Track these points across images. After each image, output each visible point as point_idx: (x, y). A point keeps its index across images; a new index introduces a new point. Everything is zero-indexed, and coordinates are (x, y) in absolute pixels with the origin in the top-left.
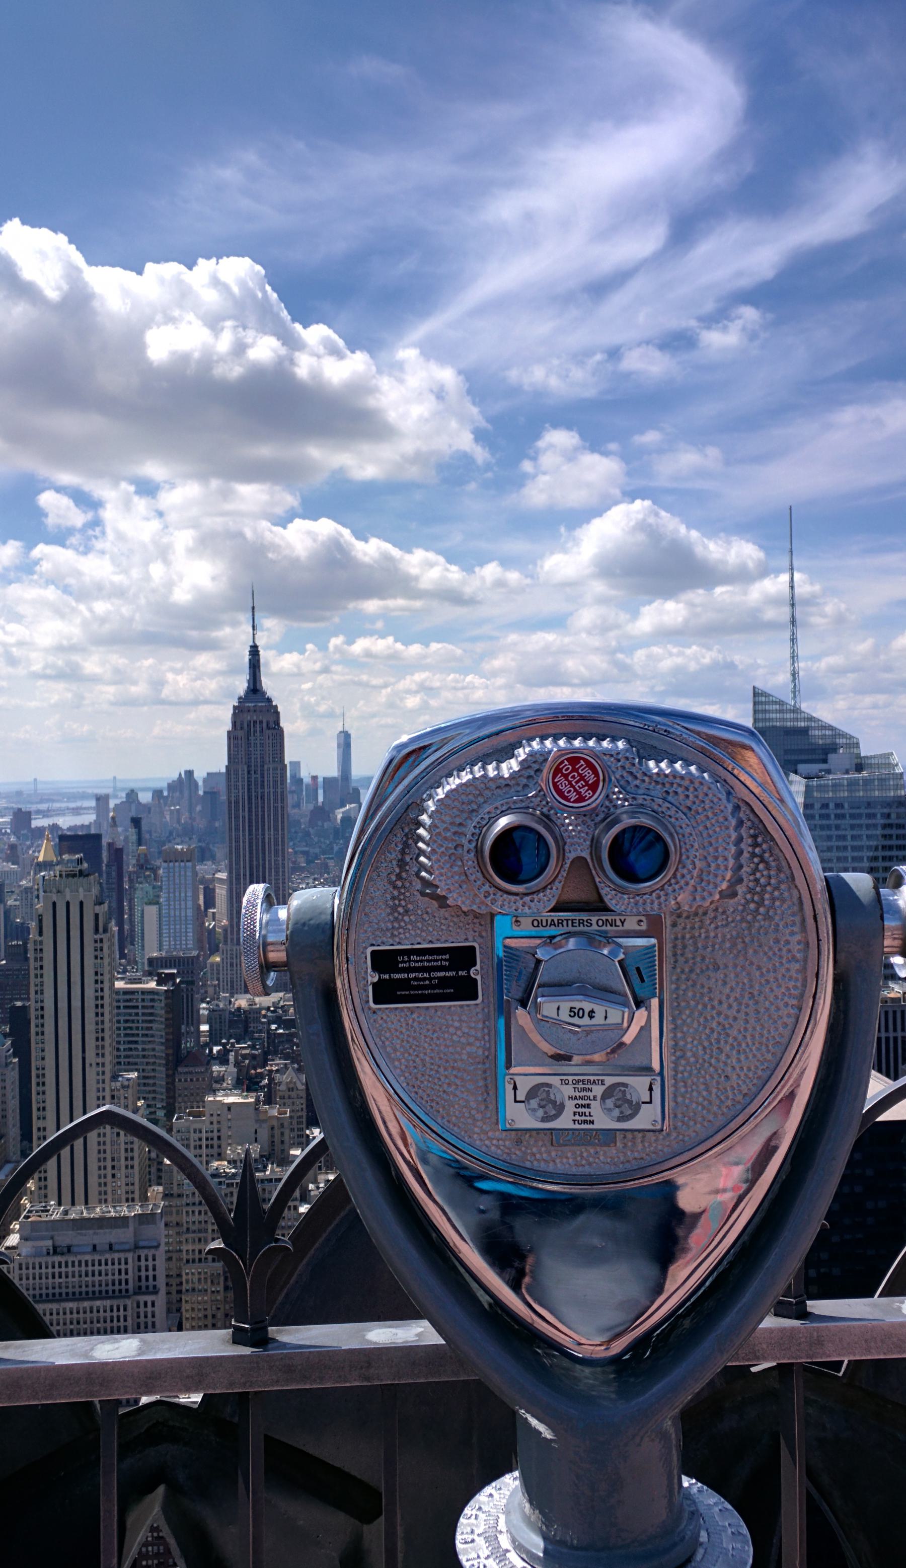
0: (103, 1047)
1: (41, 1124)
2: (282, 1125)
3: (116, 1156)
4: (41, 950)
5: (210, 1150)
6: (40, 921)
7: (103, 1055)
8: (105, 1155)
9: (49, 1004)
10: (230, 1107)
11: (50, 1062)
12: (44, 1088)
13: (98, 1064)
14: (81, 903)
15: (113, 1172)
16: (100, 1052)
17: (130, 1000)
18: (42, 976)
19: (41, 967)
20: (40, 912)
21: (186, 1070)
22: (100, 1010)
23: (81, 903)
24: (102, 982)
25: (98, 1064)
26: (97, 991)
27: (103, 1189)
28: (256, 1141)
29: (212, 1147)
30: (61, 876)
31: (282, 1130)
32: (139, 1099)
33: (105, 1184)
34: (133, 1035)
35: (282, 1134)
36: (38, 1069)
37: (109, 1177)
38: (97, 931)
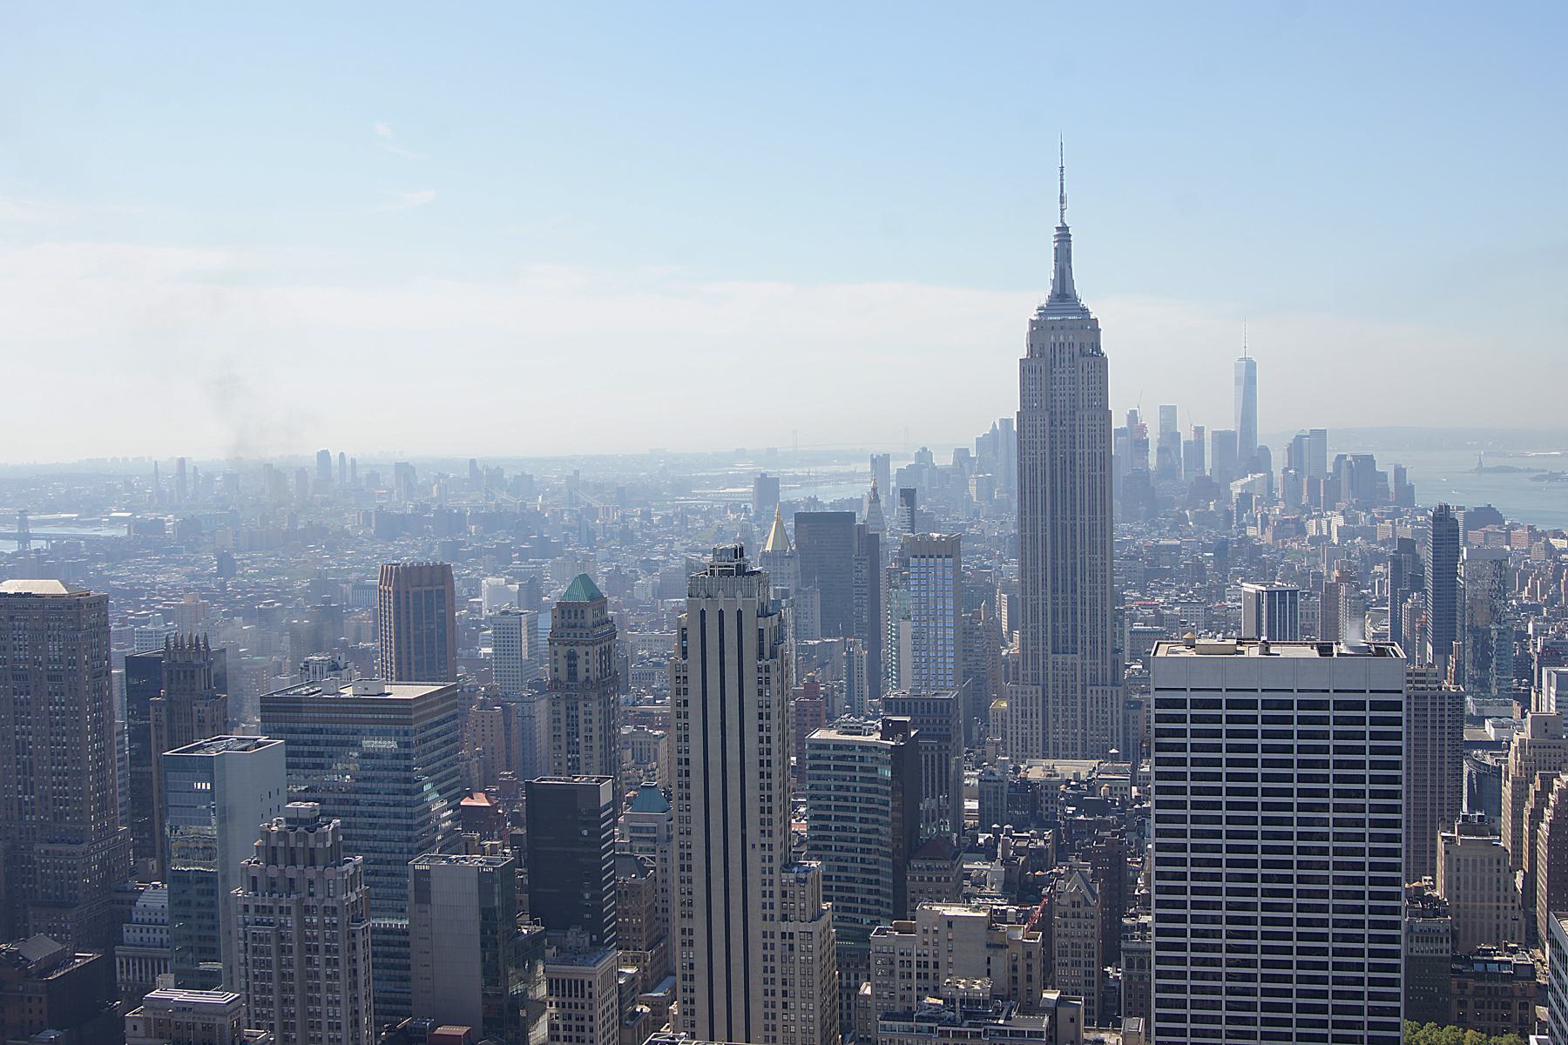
0: (770, 823)
1: (686, 924)
2: (1029, 955)
3: (788, 977)
4: (685, 678)
5: (923, 982)
6: (684, 637)
7: (770, 836)
8: (773, 976)
9: (696, 757)
10: (950, 922)
11: (698, 839)
12: (690, 874)
13: (763, 845)
14: (739, 612)
15: (785, 1000)
16: (766, 828)
17: (843, 758)
18: (686, 716)
19: (686, 703)
20: (684, 626)
21: (922, 864)
22: (765, 769)
23: (739, 612)
24: (768, 730)
25: (763, 845)
26: (761, 741)
27: (770, 1022)
28: (989, 975)
29: (926, 976)
30: (712, 572)
31: (1029, 961)
32: (827, 898)
33: (774, 1016)
34: (847, 809)
35: (1029, 966)
36: (682, 846)
37: (779, 1005)
38: (761, 655)
